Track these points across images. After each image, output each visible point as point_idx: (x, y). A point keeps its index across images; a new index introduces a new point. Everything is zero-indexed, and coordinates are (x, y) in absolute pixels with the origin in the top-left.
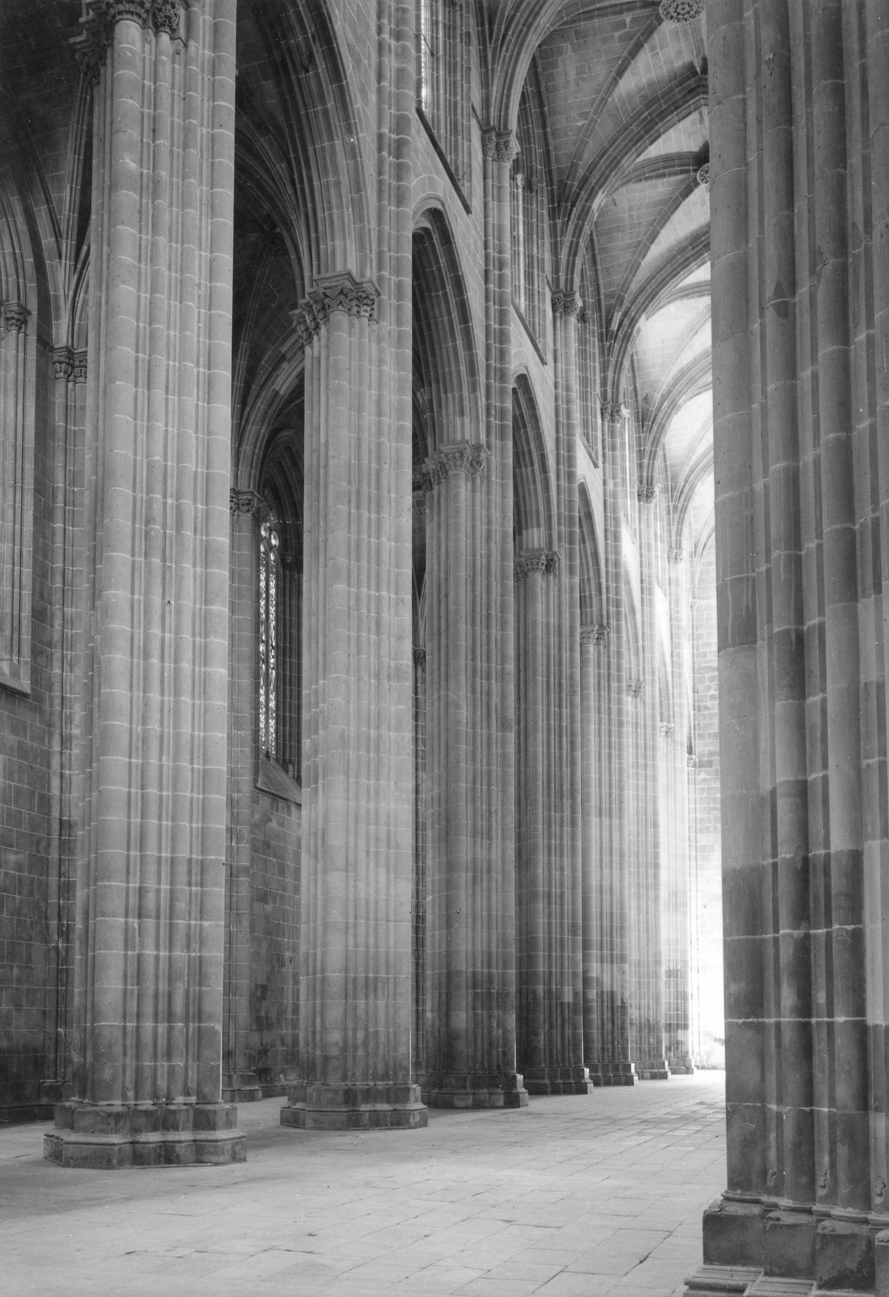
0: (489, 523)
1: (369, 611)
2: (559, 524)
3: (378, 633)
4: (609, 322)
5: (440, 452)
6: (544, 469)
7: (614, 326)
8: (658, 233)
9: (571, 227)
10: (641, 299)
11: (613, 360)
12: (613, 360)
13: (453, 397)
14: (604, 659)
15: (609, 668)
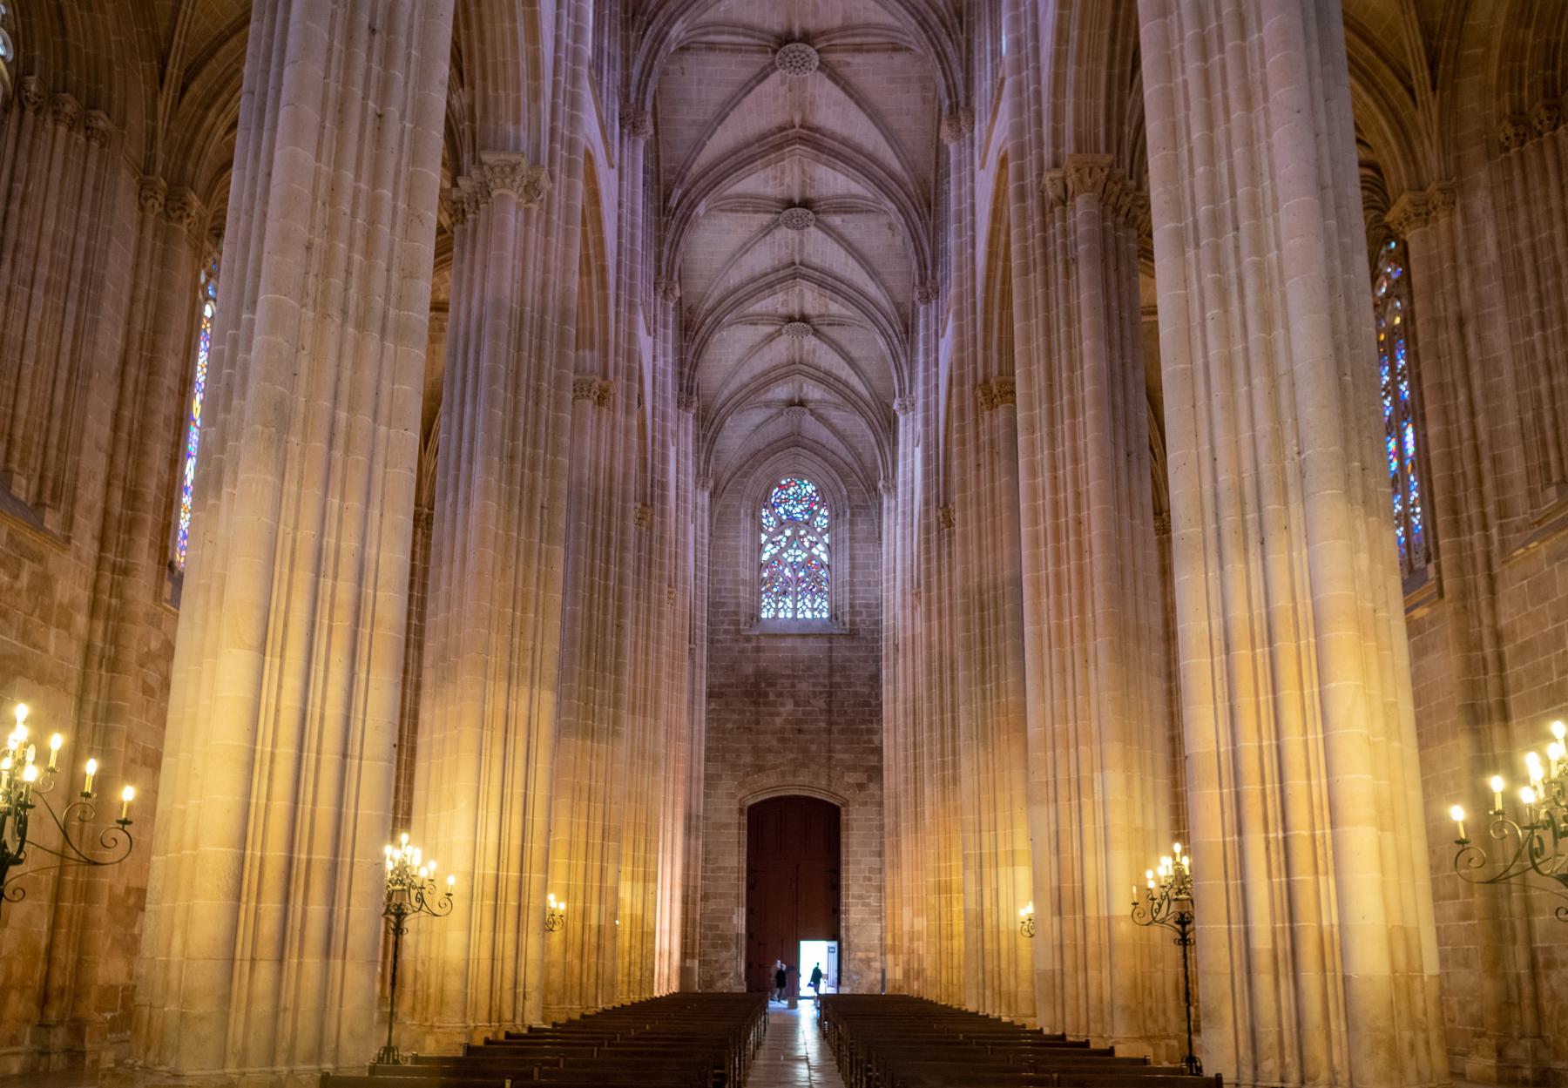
0: (546, 270)
1: (354, 214)
2: (616, 354)
3: (369, 254)
4: (667, 198)
5: (481, 163)
6: (603, 285)
7: (673, 202)
8: (727, 115)
9: (645, 46)
10: (702, 184)
11: (669, 237)
12: (669, 237)
13: (507, 96)
14: (646, 542)
15: (651, 553)
